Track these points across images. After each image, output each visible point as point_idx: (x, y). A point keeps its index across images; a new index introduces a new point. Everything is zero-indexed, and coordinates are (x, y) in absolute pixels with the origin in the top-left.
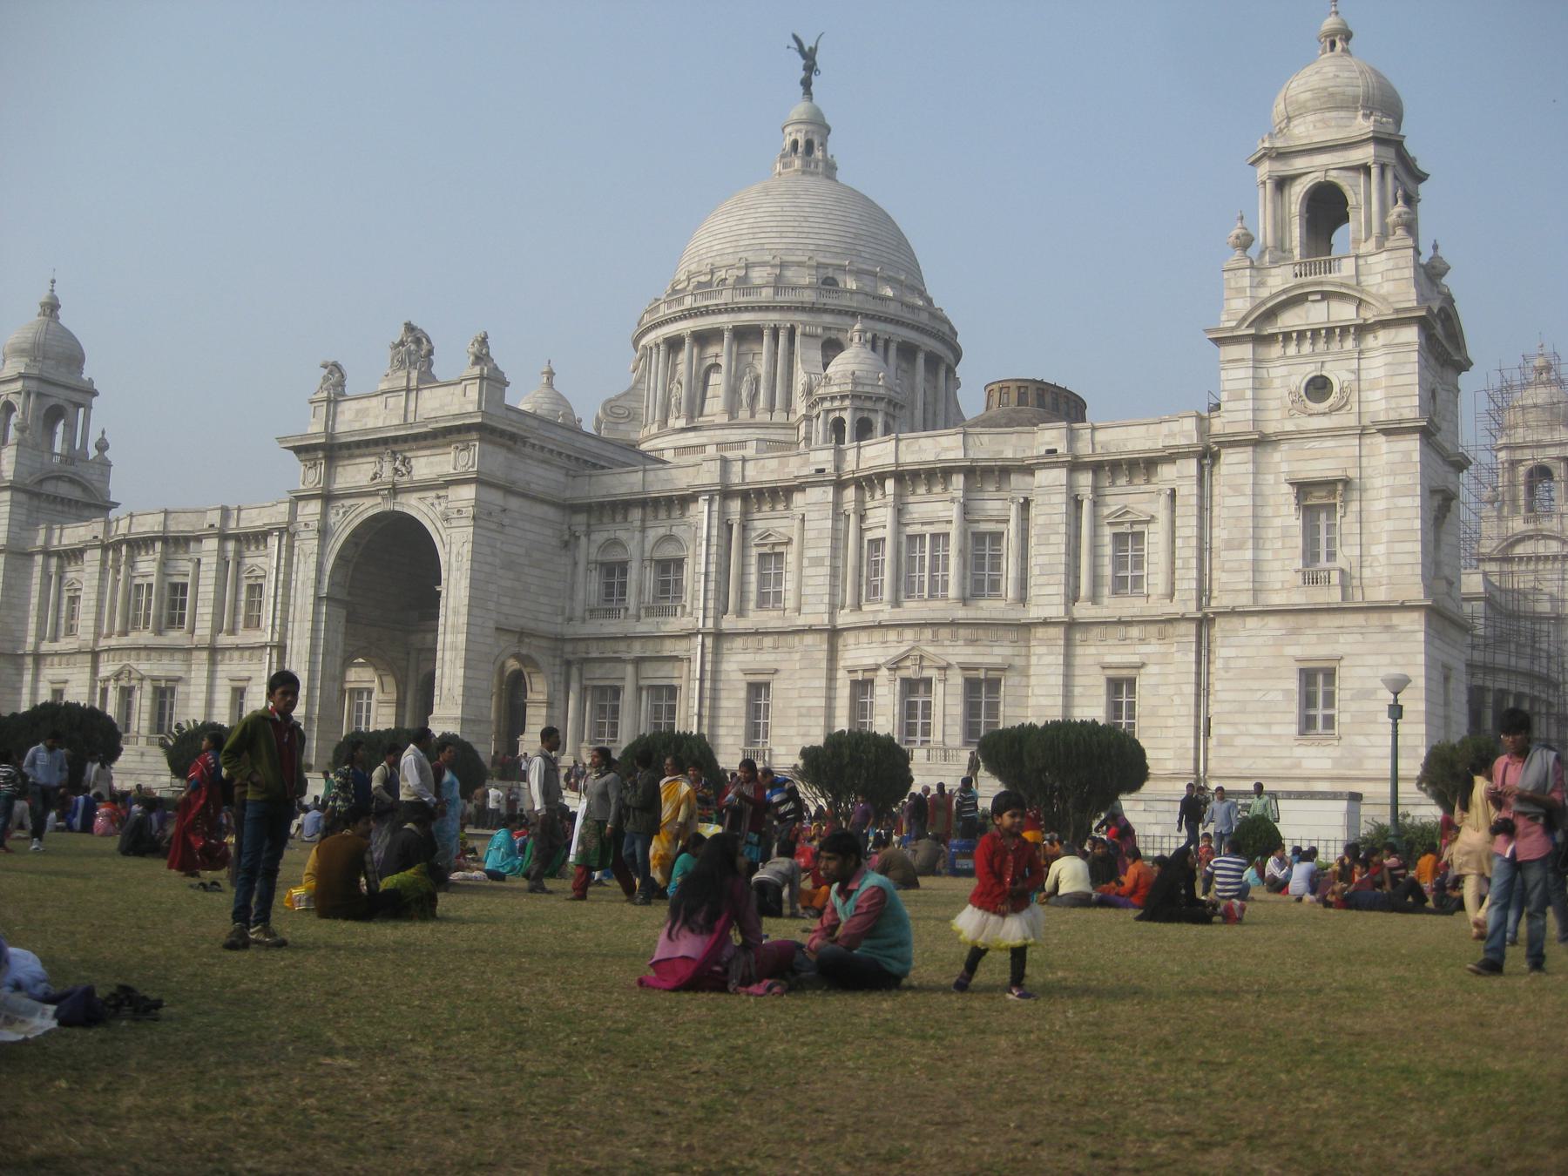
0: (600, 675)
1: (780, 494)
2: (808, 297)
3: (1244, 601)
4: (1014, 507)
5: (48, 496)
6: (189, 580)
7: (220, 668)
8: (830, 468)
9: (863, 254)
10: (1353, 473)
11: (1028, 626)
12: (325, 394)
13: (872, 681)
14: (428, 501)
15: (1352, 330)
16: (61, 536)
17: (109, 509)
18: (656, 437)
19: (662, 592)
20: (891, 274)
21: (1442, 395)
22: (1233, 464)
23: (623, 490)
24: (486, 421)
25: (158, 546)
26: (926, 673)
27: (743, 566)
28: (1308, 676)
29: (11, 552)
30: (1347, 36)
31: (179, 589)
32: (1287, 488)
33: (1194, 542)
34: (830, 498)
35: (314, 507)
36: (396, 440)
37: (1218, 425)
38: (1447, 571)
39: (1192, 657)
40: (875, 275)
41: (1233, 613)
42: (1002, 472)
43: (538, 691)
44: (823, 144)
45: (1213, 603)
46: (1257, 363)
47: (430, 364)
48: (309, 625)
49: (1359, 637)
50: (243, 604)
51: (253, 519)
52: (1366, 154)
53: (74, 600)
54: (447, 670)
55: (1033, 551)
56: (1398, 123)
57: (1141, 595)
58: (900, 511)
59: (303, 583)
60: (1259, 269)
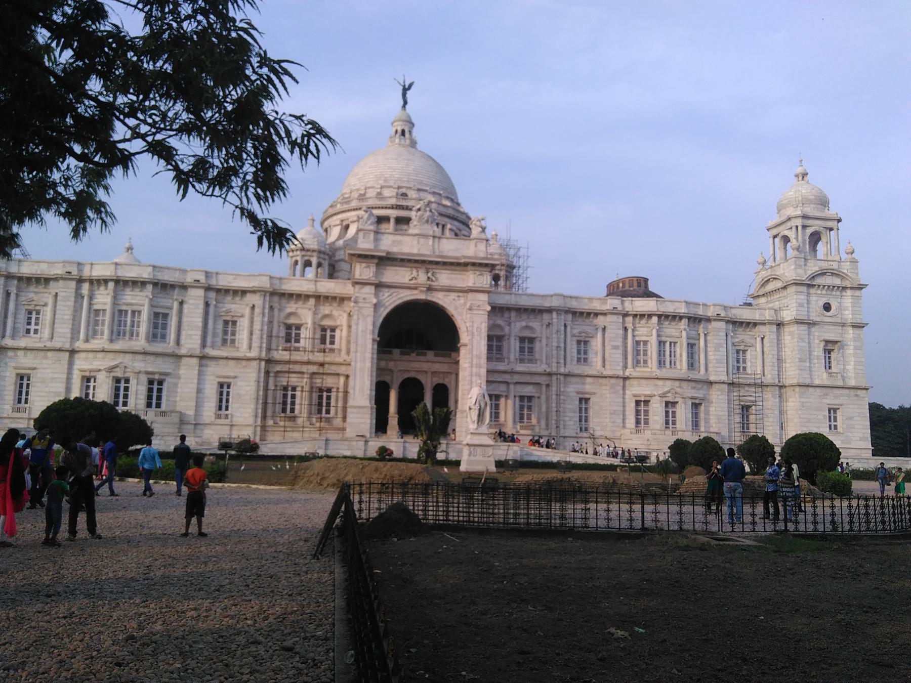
3: (808, 382)
7: (205, 369)
11: (711, 383)
26: (676, 400)
30: (804, 175)
32: (817, 341)
34: (621, 321)
36: (431, 262)
44: (410, 132)
46: (808, 294)
55: (710, 354)
59: (362, 331)
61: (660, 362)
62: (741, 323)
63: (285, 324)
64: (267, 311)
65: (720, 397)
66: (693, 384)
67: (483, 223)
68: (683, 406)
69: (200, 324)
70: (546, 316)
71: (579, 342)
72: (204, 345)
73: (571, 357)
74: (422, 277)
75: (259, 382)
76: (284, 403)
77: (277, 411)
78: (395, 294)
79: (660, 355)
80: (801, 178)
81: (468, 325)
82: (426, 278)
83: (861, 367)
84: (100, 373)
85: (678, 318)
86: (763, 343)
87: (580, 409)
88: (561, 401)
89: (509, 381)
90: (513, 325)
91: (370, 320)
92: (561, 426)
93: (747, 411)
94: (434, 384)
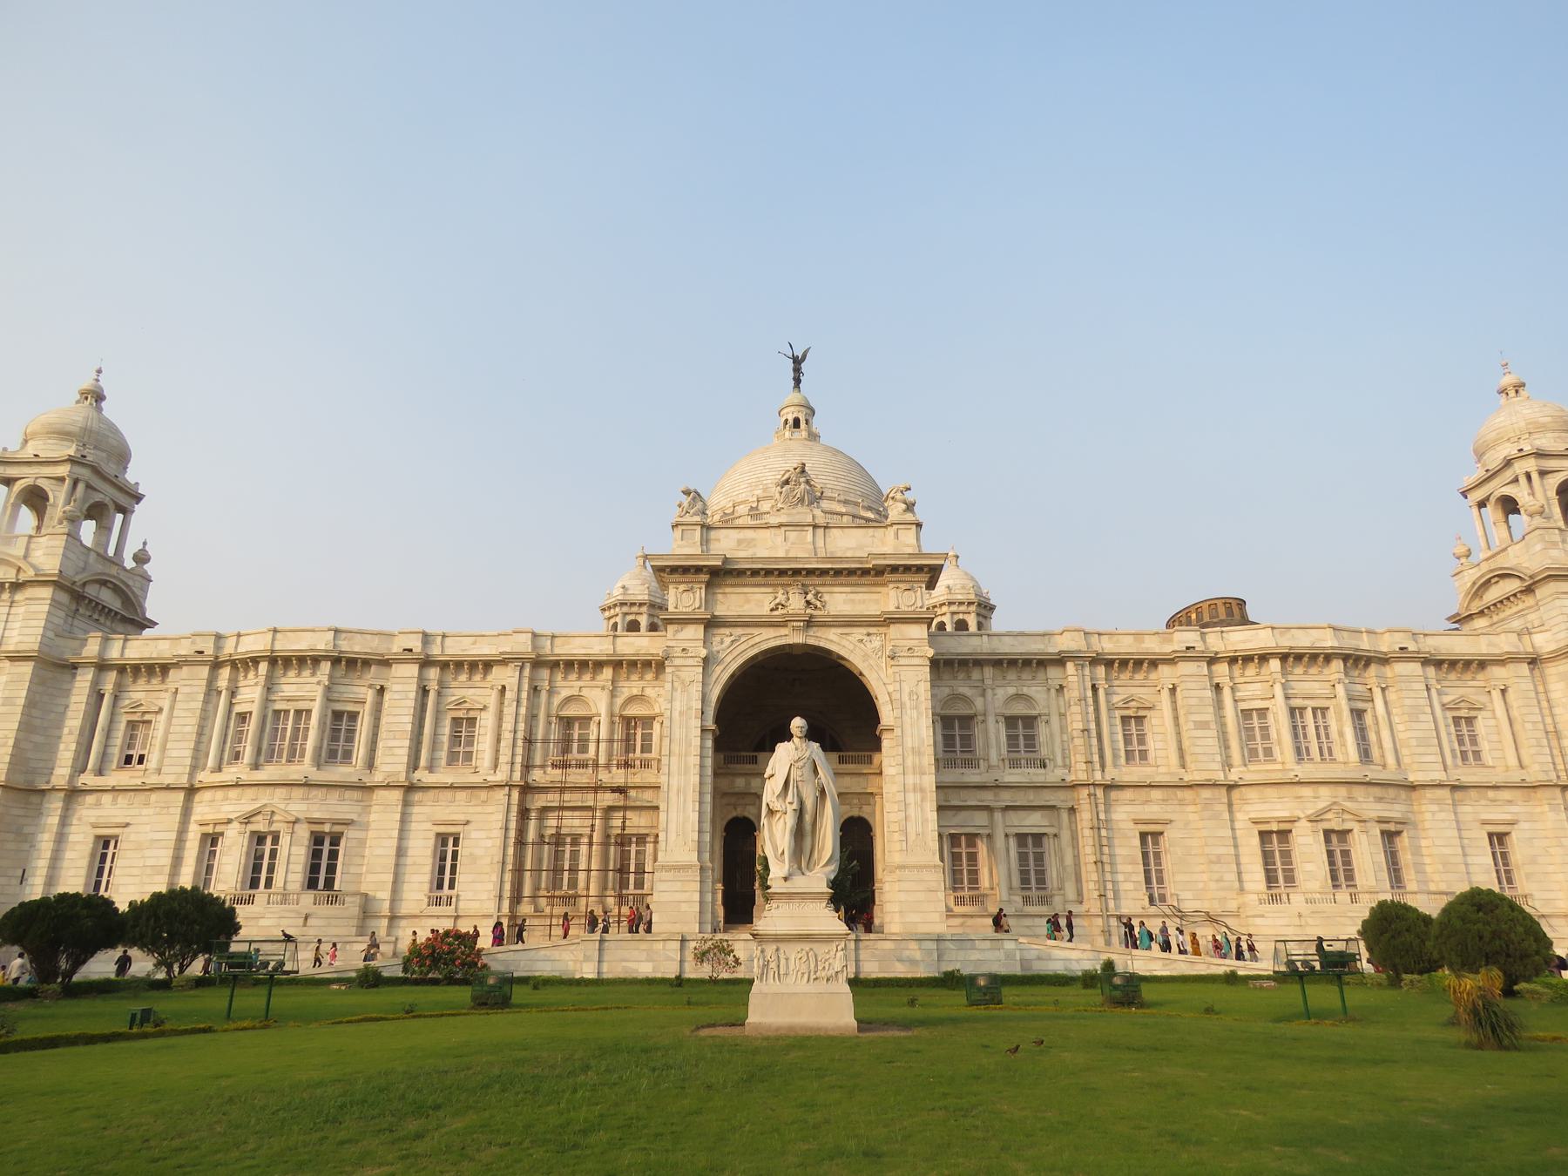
5: (91, 601)
7: (416, 810)
11: (1413, 787)
26: (1347, 826)
30: (1518, 387)
33: (1541, 727)
36: (810, 572)
57: (1483, 766)
59: (680, 712)
61: (1298, 751)
62: (1453, 664)
63: (561, 718)
64: (524, 695)
65: (1442, 815)
66: (1377, 791)
67: (909, 496)
68: (1364, 837)
69: (409, 727)
70: (1053, 672)
71: (1125, 720)
72: (414, 765)
73: (1113, 749)
74: (796, 603)
75: (507, 829)
76: (557, 871)
77: (543, 885)
78: (743, 639)
79: (1296, 736)
80: (1512, 393)
81: (891, 688)
84: (230, 826)
85: (1321, 659)
86: (1505, 703)
87: (1145, 855)
88: (1105, 842)
89: (992, 804)
90: (989, 693)
91: (695, 691)
92: (1110, 894)
93: (1501, 842)
94: (842, 820)
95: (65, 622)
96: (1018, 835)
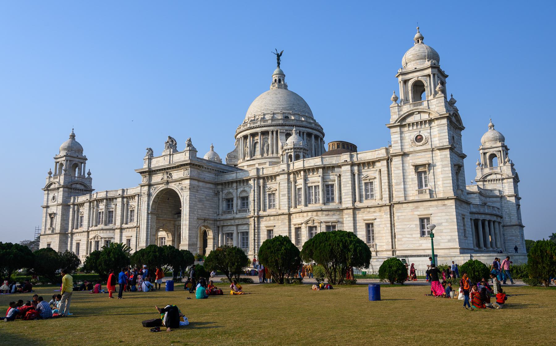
0: (226, 230)
1: (273, 177)
2: (281, 122)
3: (402, 199)
4: (336, 177)
5: (74, 189)
6: (114, 210)
7: (123, 234)
8: (286, 169)
9: (296, 109)
10: (431, 162)
12: (148, 157)
13: (300, 228)
14: (177, 185)
15: (428, 121)
16: (78, 199)
17: (92, 191)
18: (242, 162)
19: (243, 206)
20: (303, 114)
21: (456, 138)
22: (396, 161)
23: (231, 178)
24: (192, 162)
25: (105, 201)
26: (315, 225)
27: (264, 197)
28: (422, 220)
29: (64, 205)
31: (111, 213)
33: (387, 184)
34: (286, 178)
35: (146, 188)
36: (168, 169)
37: (392, 151)
38: (461, 187)
39: (389, 216)
40: (299, 115)
41: (399, 203)
42: (332, 168)
43: (210, 235)
45: (394, 201)
46: (401, 133)
47: (176, 147)
48: (146, 221)
49: (436, 208)
50: (129, 216)
51: (131, 192)
52: (429, 71)
53: (82, 217)
54: (184, 231)
55: (342, 189)
56: (438, 61)
58: (306, 180)
59: (144, 209)
60: (400, 106)
65: (349, 219)
69: (120, 214)
71: (269, 195)
82: (166, 178)
83: (448, 182)
94: (202, 231)
95: (68, 194)
96: (241, 232)
